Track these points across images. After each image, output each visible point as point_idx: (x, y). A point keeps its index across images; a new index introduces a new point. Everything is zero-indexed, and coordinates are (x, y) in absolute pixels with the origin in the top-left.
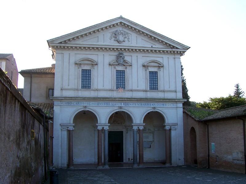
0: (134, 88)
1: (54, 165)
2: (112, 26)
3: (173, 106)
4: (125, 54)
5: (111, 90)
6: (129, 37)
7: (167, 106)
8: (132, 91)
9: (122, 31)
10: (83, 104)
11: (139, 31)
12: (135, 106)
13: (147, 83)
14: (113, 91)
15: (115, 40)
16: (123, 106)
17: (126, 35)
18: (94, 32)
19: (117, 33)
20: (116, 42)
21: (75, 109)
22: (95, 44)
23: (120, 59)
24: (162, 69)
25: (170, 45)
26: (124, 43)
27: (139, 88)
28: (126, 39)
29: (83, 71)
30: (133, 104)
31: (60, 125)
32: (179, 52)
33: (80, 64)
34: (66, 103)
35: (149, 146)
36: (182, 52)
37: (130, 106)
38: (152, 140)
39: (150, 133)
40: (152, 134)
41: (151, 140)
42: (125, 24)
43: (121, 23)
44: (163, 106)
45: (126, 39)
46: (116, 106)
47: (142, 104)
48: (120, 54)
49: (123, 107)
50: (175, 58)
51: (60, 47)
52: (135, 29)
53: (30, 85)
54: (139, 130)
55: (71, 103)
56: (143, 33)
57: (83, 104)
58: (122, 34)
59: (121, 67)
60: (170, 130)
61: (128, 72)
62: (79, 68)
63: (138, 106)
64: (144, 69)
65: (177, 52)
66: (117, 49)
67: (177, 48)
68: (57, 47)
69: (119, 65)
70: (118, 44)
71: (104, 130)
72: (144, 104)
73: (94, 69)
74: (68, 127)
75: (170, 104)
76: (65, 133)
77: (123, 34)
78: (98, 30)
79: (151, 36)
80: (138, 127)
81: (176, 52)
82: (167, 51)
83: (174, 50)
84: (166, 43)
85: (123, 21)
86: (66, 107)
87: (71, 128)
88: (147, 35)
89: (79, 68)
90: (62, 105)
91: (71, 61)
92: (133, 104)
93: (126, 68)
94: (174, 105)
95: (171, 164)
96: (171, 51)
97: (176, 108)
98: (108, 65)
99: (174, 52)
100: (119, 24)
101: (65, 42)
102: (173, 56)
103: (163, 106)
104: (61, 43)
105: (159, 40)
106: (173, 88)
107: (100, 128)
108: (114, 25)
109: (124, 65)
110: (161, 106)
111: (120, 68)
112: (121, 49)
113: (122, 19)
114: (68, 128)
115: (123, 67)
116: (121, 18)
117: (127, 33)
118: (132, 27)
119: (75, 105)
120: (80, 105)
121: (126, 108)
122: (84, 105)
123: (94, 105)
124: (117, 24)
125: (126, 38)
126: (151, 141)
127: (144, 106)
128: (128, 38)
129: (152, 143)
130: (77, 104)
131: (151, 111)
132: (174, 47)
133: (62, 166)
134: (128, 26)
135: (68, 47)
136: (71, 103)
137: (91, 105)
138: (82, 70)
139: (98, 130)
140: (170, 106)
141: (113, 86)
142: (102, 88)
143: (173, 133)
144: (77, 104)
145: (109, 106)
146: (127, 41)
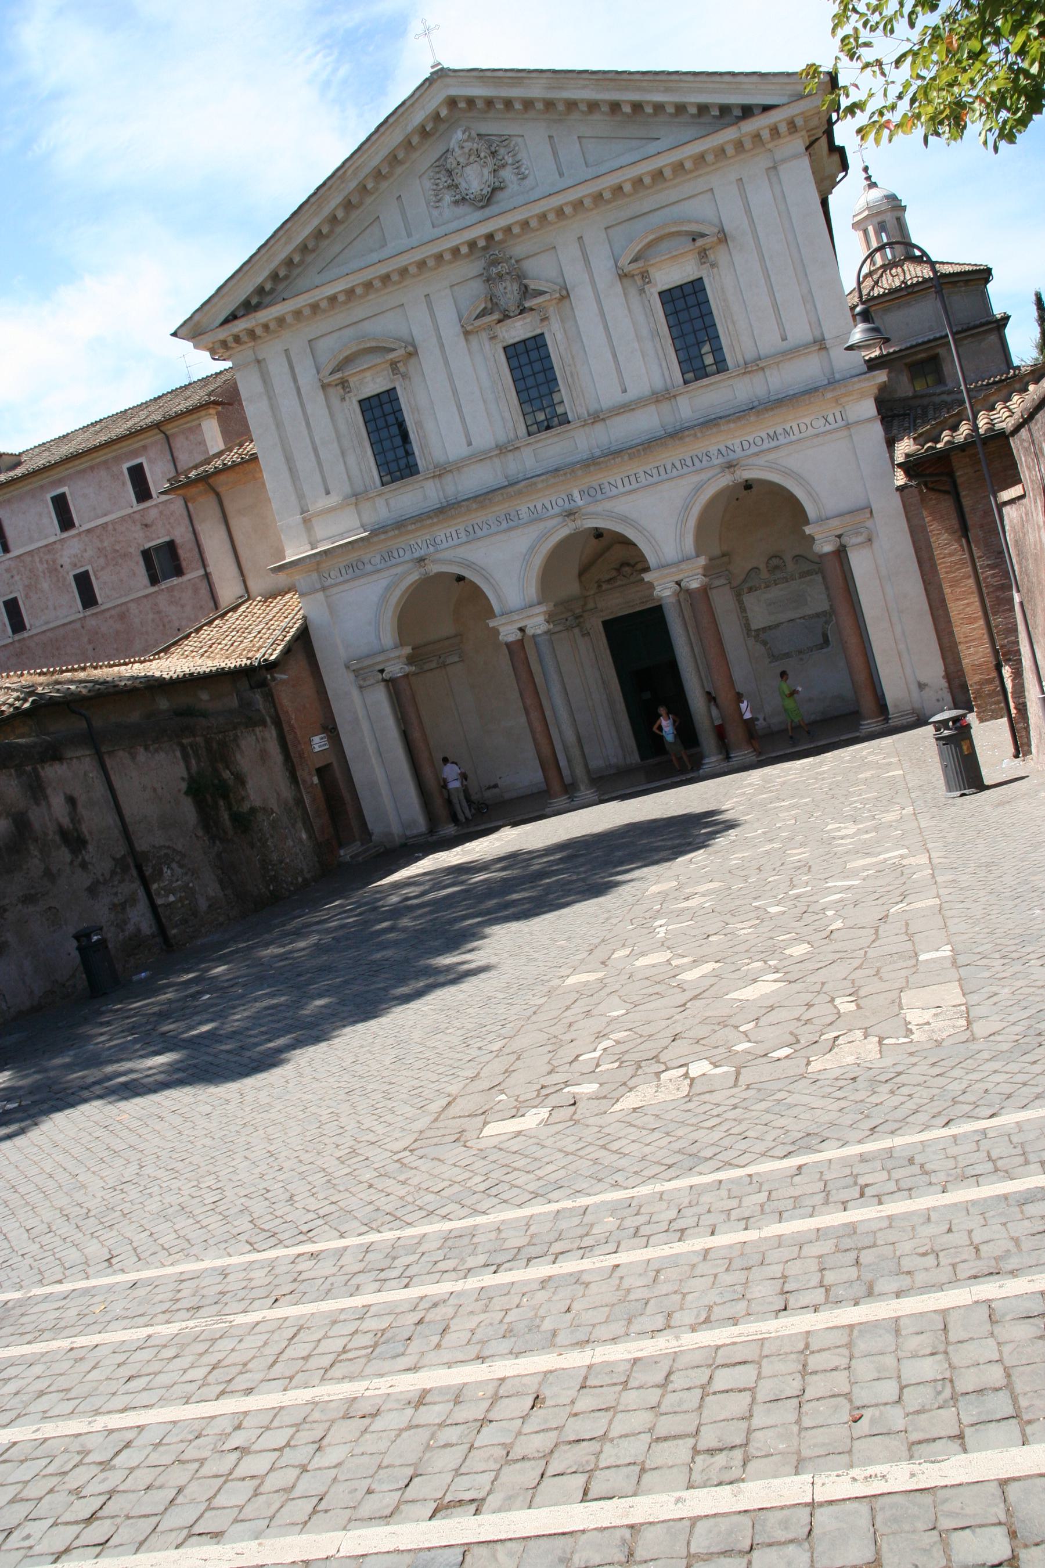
0: (606, 402)
1: (374, 838)
2: (415, 140)
3: (828, 427)
4: (519, 249)
5: (503, 450)
6: (518, 157)
7: (793, 438)
8: (597, 418)
9: (468, 145)
10: (408, 553)
11: (549, 104)
12: (635, 485)
13: (661, 355)
14: (517, 453)
15: (456, 203)
16: (580, 503)
17: (502, 151)
18: (348, 205)
19: (451, 163)
20: (462, 209)
21: (384, 583)
22: (375, 257)
23: (501, 288)
24: (720, 255)
25: (725, 110)
26: (500, 196)
27: (633, 394)
28: (507, 174)
29: (367, 405)
30: (626, 480)
31: (347, 667)
32: (783, 128)
33: (342, 378)
34: (343, 571)
35: (821, 641)
36: (799, 122)
37: (615, 491)
38: (825, 606)
39: (809, 573)
40: (818, 578)
41: (820, 610)
42: (471, 101)
43: (452, 102)
44: (773, 444)
45: (507, 174)
46: (548, 514)
47: (669, 468)
48: (495, 263)
49: (580, 508)
50: (775, 168)
51: (237, 339)
52: (528, 104)
53: (223, 528)
54: (688, 591)
55: (361, 566)
56: (572, 105)
57: (408, 553)
58: (472, 159)
59: (518, 324)
60: (841, 553)
61: (559, 336)
62: (343, 399)
63: (650, 480)
64: (633, 292)
65: (775, 131)
66: (472, 245)
67: (766, 108)
68: (224, 344)
69: (508, 317)
70: (478, 215)
71: (534, 636)
72: (678, 465)
73: (405, 376)
74: (380, 667)
75: (807, 421)
76: (380, 696)
77: (482, 155)
78: (363, 189)
79: (615, 107)
80: (678, 583)
81: (766, 135)
82: (721, 152)
83: (749, 126)
84: (703, 109)
85: (454, 92)
86: (346, 586)
87: (396, 669)
88: (593, 106)
89: (343, 399)
90: (330, 582)
91: (301, 382)
92: (626, 480)
93: (542, 320)
94: (831, 419)
95: (887, 720)
96: (739, 145)
97: (845, 433)
98: (462, 336)
99: (757, 136)
100: (444, 113)
101: (248, 307)
102: (761, 162)
103: (773, 444)
104: (233, 317)
105: (659, 107)
106: (800, 332)
107: (508, 633)
108: (424, 132)
109: (532, 309)
110: (766, 446)
111: (518, 330)
112: (490, 237)
113: (448, 80)
114: (382, 671)
115: (528, 320)
116: (440, 75)
117: (505, 140)
118: (508, 103)
119: (379, 567)
120: (401, 560)
121: (599, 508)
122: (417, 555)
123: (456, 541)
124: (436, 117)
125: (503, 166)
126: (824, 613)
127: (681, 472)
128: (510, 161)
129: (827, 622)
130: (387, 559)
131: (564, 532)
132: (747, 111)
133: (408, 833)
134: (490, 103)
135: (266, 327)
136: (361, 566)
137: (445, 545)
138: (360, 402)
139: (508, 645)
140: (811, 431)
141: (510, 425)
142: (463, 451)
143: (860, 563)
144: (387, 559)
145: (521, 522)
146: (514, 178)
